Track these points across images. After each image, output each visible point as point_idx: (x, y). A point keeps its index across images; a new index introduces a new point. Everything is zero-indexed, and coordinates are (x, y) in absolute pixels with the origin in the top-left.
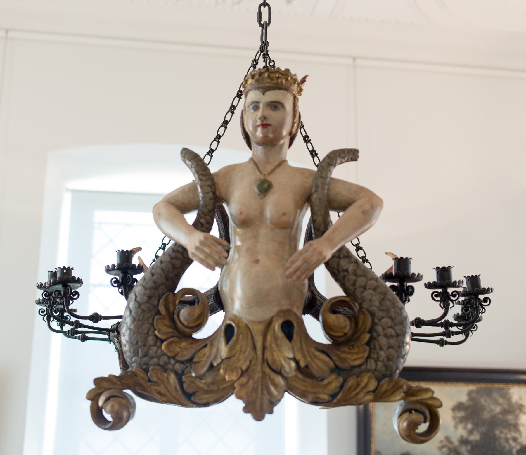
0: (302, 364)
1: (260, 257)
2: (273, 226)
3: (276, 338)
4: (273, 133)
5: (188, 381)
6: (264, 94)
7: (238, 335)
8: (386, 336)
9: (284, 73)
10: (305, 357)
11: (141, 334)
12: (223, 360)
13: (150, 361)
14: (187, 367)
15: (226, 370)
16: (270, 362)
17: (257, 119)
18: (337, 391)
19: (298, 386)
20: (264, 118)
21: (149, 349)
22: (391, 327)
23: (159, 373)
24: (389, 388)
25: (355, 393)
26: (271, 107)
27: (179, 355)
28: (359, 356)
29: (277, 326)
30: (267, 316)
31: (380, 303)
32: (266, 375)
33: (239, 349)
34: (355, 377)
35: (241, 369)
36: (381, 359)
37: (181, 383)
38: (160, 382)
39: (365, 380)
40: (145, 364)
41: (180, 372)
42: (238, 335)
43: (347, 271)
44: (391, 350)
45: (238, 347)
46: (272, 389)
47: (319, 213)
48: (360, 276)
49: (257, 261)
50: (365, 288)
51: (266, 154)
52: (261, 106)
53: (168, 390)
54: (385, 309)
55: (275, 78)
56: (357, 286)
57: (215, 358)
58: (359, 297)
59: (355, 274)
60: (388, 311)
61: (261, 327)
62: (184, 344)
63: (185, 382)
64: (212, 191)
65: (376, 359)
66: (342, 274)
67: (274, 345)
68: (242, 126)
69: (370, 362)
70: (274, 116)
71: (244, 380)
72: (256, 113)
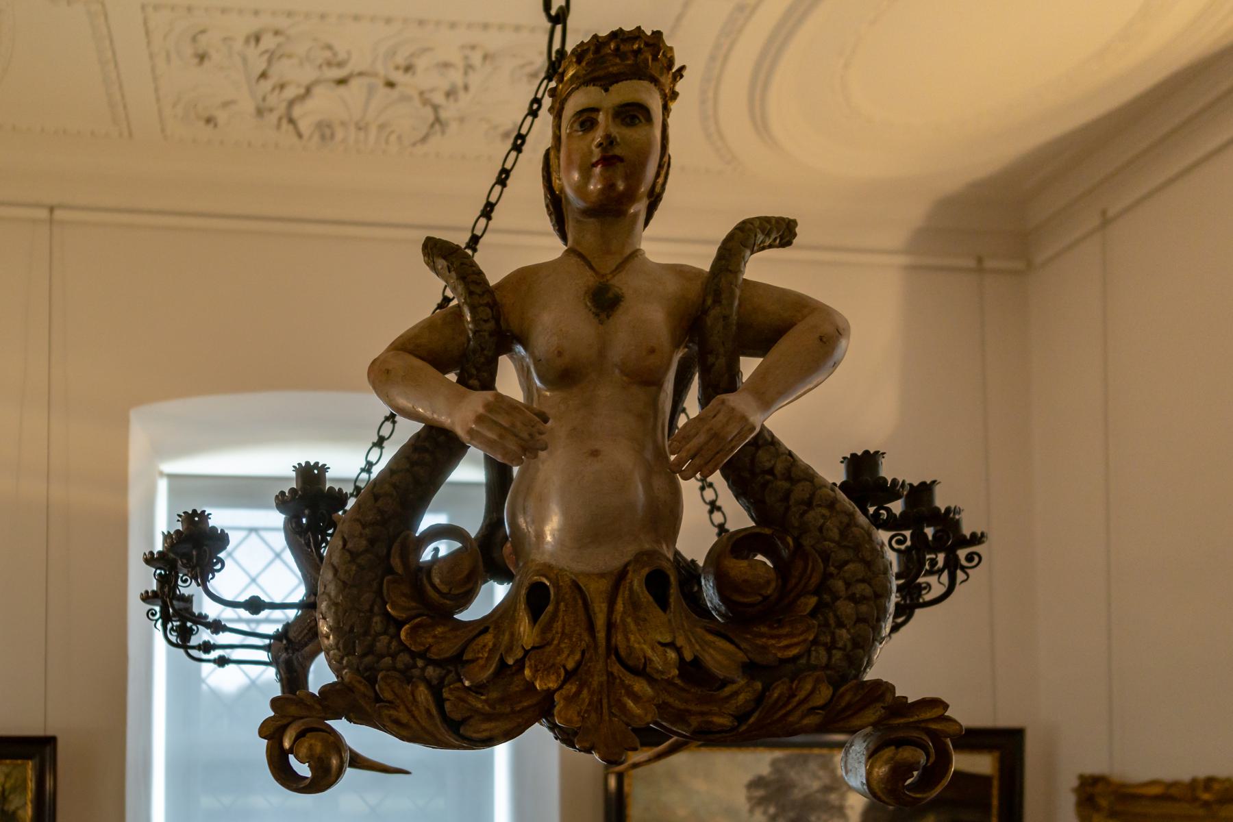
0: (688, 656)
3: (634, 605)
5: (452, 698)
7: (558, 604)
8: (852, 598)
9: (651, 42)
12: (526, 652)
13: (378, 662)
14: (449, 672)
15: (535, 671)
16: (623, 653)
27: (434, 649)
28: (795, 640)
29: (637, 581)
30: (617, 563)
31: (842, 533)
32: (615, 678)
33: (560, 630)
35: (564, 667)
36: (840, 645)
37: (440, 702)
40: (366, 669)
41: (435, 682)
42: (558, 604)
45: (558, 626)
46: (630, 704)
49: (595, 453)
50: (809, 504)
52: (601, 117)
53: (413, 717)
54: (851, 544)
55: (629, 55)
56: (792, 502)
60: (857, 548)
61: (604, 585)
67: (629, 620)
71: (572, 688)
72: (590, 136)
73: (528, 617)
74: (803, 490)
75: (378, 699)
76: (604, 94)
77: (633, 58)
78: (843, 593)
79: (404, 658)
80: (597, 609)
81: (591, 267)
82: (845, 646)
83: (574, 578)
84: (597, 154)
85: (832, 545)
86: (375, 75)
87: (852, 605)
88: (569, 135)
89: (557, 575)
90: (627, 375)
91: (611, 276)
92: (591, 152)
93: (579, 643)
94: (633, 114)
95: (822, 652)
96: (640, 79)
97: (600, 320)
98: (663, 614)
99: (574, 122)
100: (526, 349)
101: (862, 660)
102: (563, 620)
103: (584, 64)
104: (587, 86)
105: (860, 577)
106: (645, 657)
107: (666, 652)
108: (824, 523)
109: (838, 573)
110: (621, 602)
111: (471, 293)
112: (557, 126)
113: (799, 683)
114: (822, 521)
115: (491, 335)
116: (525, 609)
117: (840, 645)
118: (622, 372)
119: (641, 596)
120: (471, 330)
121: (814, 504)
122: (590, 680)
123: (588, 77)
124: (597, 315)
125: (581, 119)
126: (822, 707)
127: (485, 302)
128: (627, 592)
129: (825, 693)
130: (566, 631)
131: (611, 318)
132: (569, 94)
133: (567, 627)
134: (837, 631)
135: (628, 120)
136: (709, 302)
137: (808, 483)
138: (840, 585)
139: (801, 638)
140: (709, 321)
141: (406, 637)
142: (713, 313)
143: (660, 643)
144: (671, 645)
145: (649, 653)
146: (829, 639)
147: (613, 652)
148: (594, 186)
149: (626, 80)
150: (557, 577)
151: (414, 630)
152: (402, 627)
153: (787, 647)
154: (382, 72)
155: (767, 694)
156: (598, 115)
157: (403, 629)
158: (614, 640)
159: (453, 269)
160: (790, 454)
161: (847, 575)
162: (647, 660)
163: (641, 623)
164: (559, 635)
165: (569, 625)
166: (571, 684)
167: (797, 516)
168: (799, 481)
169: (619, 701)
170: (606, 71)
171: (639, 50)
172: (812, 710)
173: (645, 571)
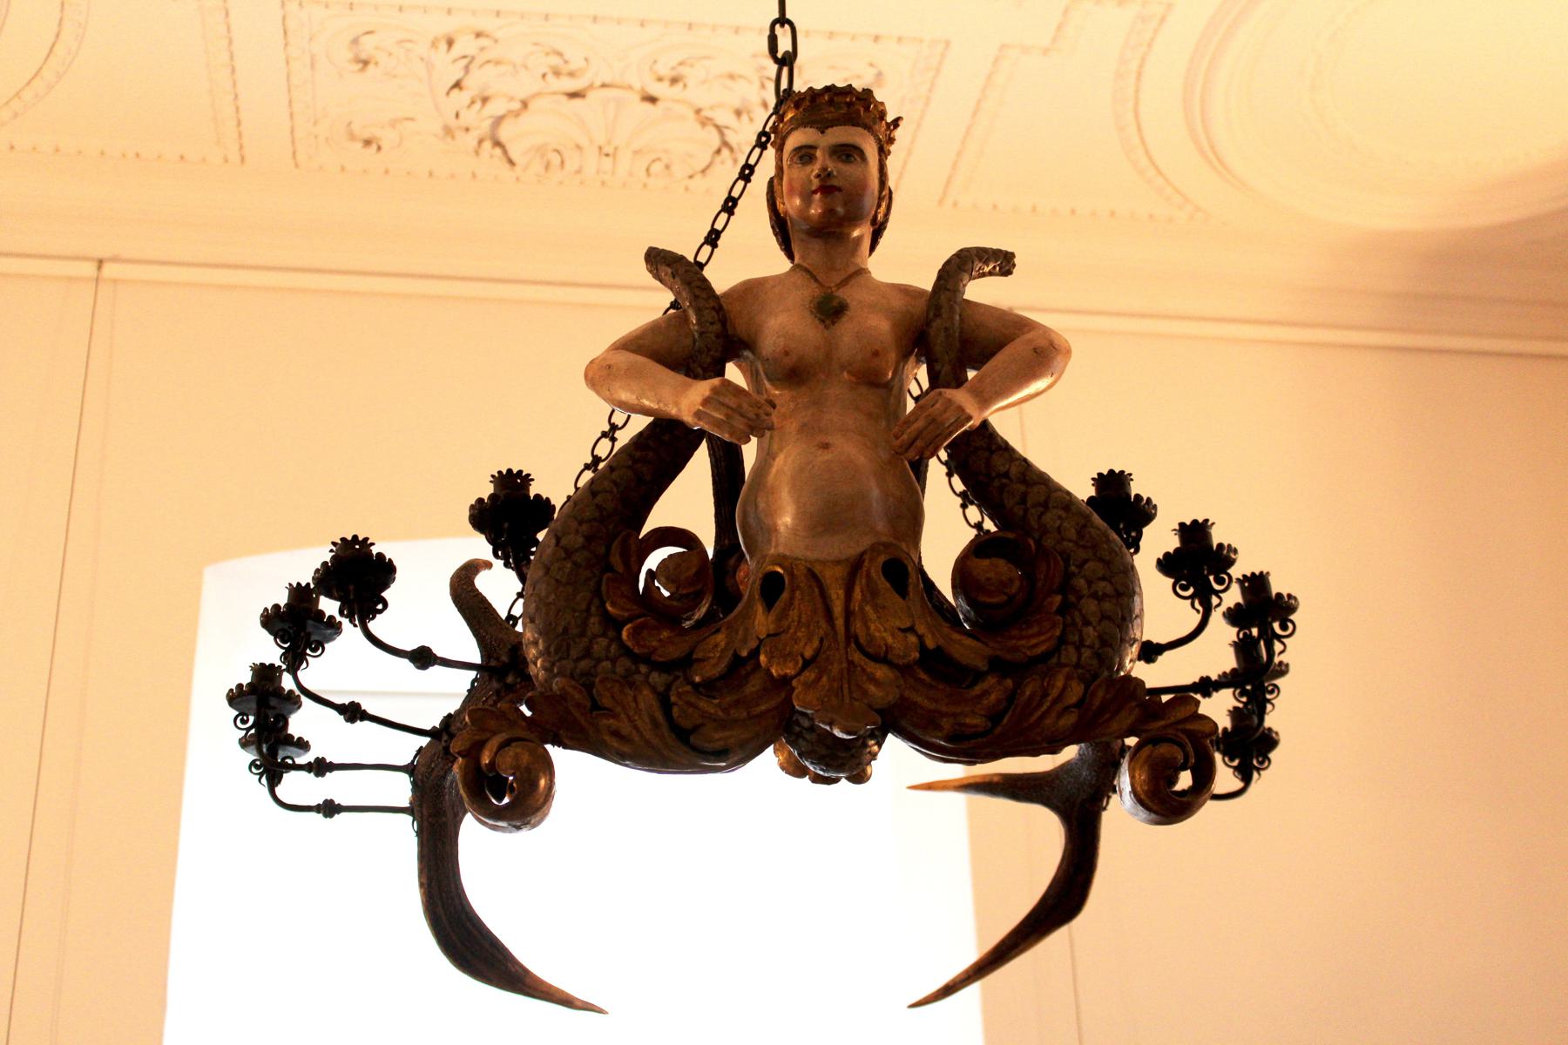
1: (829, 439)
2: (853, 379)
3: (872, 593)
4: (845, 204)
5: (680, 703)
6: (823, 132)
7: (793, 591)
8: (1094, 596)
11: (574, 611)
12: (761, 641)
13: (595, 667)
14: (677, 678)
15: (771, 658)
16: (862, 641)
17: (812, 177)
19: (919, 699)
20: (825, 175)
21: (591, 642)
22: (1103, 579)
23: (617, 688)
26: (839, 157)
28: (1043, 638)
29: (875, 569)
30: (852, 551)
32: (855, 667)
33: (796, 618)
35: (802, 656)
36: (1088, 643)
37: (666, 705)
38: (619, 709)
39: (1060, 683)
40: (583, 674)
41: (661, 689)
42: (793, 591)
43: (1006, 475)
44: (1106, 623)
45: (794, 614)
50: (1045, 505)
52: (818, 153)
53: (636, 728)
54: (1089, 544)
57: (745, 641)
58: (1034, 524)
60: (1095, 547)
61: (840, 572)
62: (665, 634)
63: (675, 704)
64: (720, 320)
65: (1077, 643)
66: (996, 483)
67: (868, 608)
69: (1066, 649)
70: (844, 172)
71: (810, 675)
72: (808, 168)
74: (1038, 492)
75: (596, 706)
76: (820, 135)
78: (1085, 592)
79: (624, 664)
80: (834, 596)
81: (816, 280)
83: (808, 565)
85: (1071, 544)
86: (630, 87)
88: (789, 167)
90: (854, 376)
92: (811, 181)
93: (817, 630)
94: (848, 153)
95: (1071, 649)
96: (853, 125)
98: (901, 600)
99: (795, 155)
100: (753, 353)
101: (1112, 659)
102: (799, 608)
103: (801, 110)
105: (1100, 575)
106: (886, 645)
108: (1062, 523)
109: (1079, 573)
111: (696, 297)
112: (779, 159)
113: (1050, 680)
114: (1059, 522)
115: (717, 336)
117: (1088, 643)
118: (849, 372)
119: (879, 582)
120: (696, 331)
121: (1050, 505)
122: (830, 667)
124: (823, 321)
126: (1075, 706)
128: (864, 580)
129: (1076, 692)
130: (803, 620)
131: (836, 325)
132: (789, 133)
134: (1084, 629)
136: (931, 315)
137: (1042, 486)
138: (1081, 583)
139: (1048, 635)
140: (932, 332)
141: (628, 637)
142: (934, 324)
143: (900, 629)
144: (911, 629)
145: (890, 640)
146: (1076, 638)
148: (815, 211)
151: (635, 633)
152: (624, 627)
153: (1035, 646)
154: (637, 86)
155: (1019, 691)
156: (816, 152)
157: (625, 629)
160: (1025, 460)
163: (881, 611)
164: (796, 624)
167: (1036, 517)
168: (1035, 484)
169: (859, 687)
171: (850, 104)
172: (1066, 709)
173: (882, 559)
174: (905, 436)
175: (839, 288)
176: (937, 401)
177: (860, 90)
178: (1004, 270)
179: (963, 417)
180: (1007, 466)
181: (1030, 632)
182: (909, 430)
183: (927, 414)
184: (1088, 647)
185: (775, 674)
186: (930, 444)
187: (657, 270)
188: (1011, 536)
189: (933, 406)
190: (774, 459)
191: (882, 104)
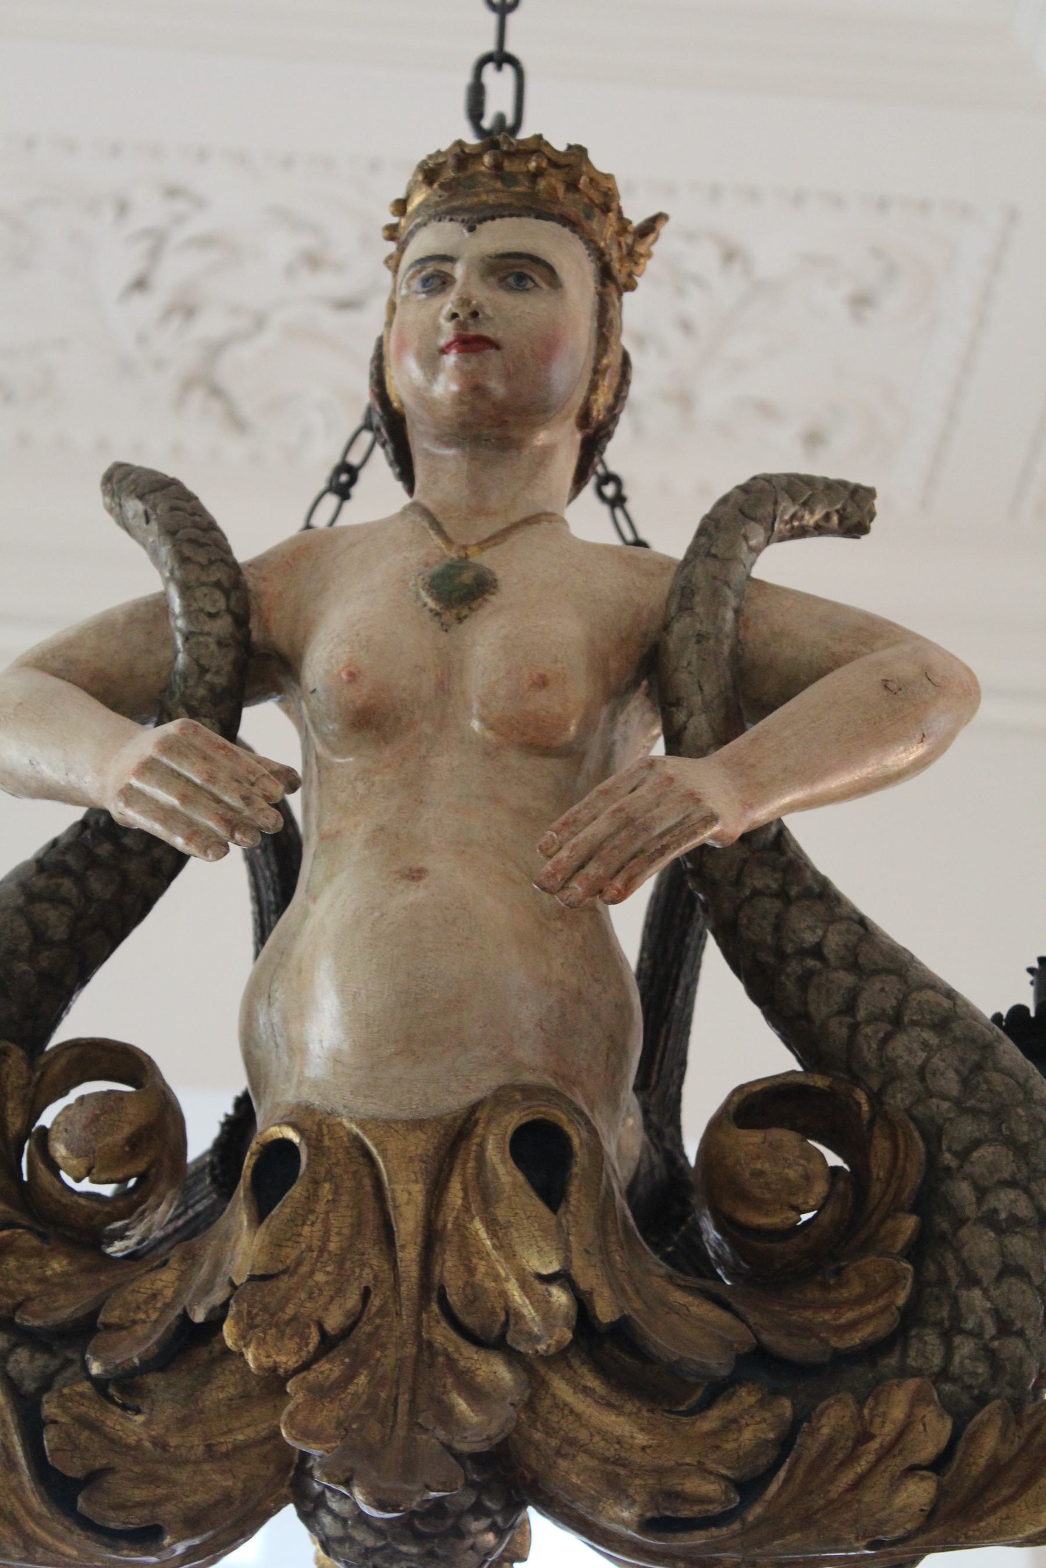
0: (605, 1311)
1: (428, 862)
4: (508, 377)
6: (472, 229)
7: (316, 1182)
8: (990, 1220)
9: (563, 161)
10: (619, 1291)
16: (454, 1299)
17: (442, 321)
18: (763, 1461)
22: (1011, 1184)
24: (1008, 1451)
25: (847, 1478)
26: (502, 279)
27: (35, 1306)
31: (965, 1082)
33: (316, 1243)
34: (849, 1398)
35: (320, 1326)
36: (970, 1324)
43: (817, 951)
46: (461, 1405)
47: (697, 700)
48: (876, 972)
49: (416, 875)
50: (897, 1021)
51: (473, 481)
54: (985, 1106)
55: (520, 177)
56: (861, 1014)
57: (207, 1288)
58: (869, 1053)
59: (854, 966)
60: (999, 1114)
61: (421, 1143)
62: (57, 1265)
64: (229, 610)
66: (794, 967)
68: (376, 363)
69: (920, 1338)
72: (436, 302)
73: (248, 1215)
74: (882, 990)
76: (467, 234)
77: (527, 184)
78: (971, 1211)
80: (402, 1197)
82: (981, 1325)
84: (448, 331)
85: (946, 1105)
87: (992, 1234)
89: (320, 1124)
91: (475, 549)
92: (438, 330)
93: (357, 1270)
97: (442, 624)
99: (412, 277)
102: (326, 1222)
103: (436, 186)
104: (440, 220)
105: (1006, 1175)
107: (550, 1295)
110: (458, 1186)
111: (183, 560)
114: (924, 1055)
116: (245, 1197)
117: (970, 1324)
120: (180, 630)
121: (906, 1019)
122: (378, 1354)
123: (444, 207)
125: (424, 273)
127: (213, 579)
128: (471, 1164)
130: (332, 1246)
131: (466, 623)
133: (334, 1238)
135: (511, 280)
136: (674, 608)
138: (963, 1191)
140: (673, 642)
147: (434, 1295)
149: (511, 216)
150: (320, 1129)
158: (437, 1269)
159: (154, 517)
161: (978, 1170)
162: (512, 1314)
164: (315, 1254)
165: (339, 1234)
166: (331, 1361)
167: (874, 1045)
169: (441, 1404)
170: (475, 199)
173: (514, 1119)
174: (564, 854)
175: (482, 549)
176: (643, 781)
177: (561, 147)
178: (848, 523)
179: (696, 816)
180: (820, 932)
181: (845, 1293)
182: (574, 841)
183: (615, 806)
184: (970, 1333)
185: (252, 1365)
186: (618, 872)
187: (121, 506)
188: (820, 1081)
189: (634, 790)
190: (315, 899)
191: (609, 177)
